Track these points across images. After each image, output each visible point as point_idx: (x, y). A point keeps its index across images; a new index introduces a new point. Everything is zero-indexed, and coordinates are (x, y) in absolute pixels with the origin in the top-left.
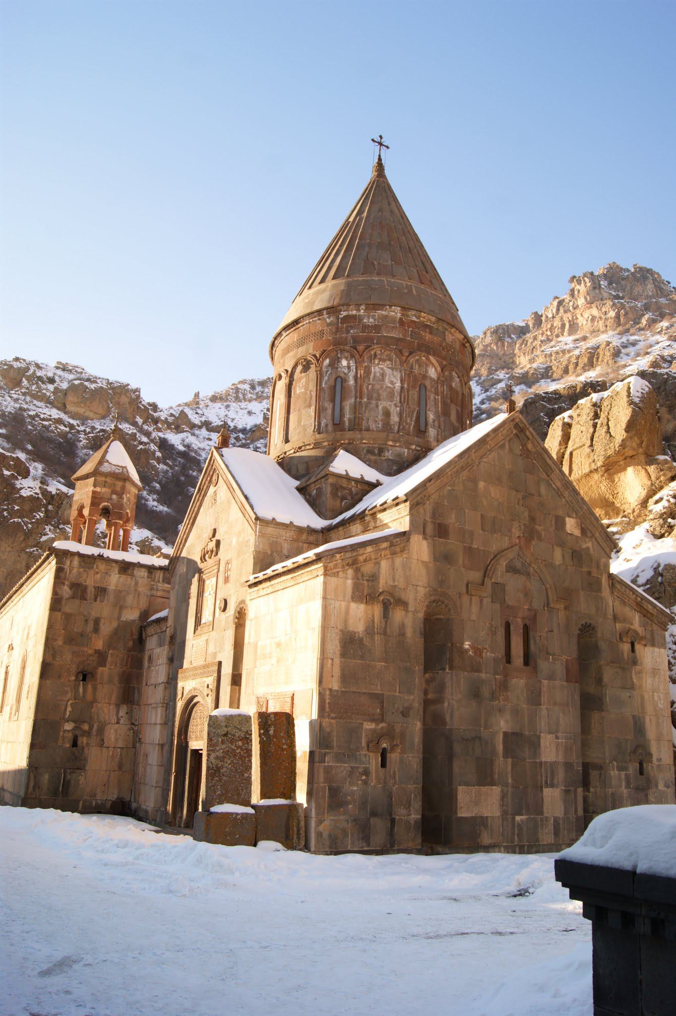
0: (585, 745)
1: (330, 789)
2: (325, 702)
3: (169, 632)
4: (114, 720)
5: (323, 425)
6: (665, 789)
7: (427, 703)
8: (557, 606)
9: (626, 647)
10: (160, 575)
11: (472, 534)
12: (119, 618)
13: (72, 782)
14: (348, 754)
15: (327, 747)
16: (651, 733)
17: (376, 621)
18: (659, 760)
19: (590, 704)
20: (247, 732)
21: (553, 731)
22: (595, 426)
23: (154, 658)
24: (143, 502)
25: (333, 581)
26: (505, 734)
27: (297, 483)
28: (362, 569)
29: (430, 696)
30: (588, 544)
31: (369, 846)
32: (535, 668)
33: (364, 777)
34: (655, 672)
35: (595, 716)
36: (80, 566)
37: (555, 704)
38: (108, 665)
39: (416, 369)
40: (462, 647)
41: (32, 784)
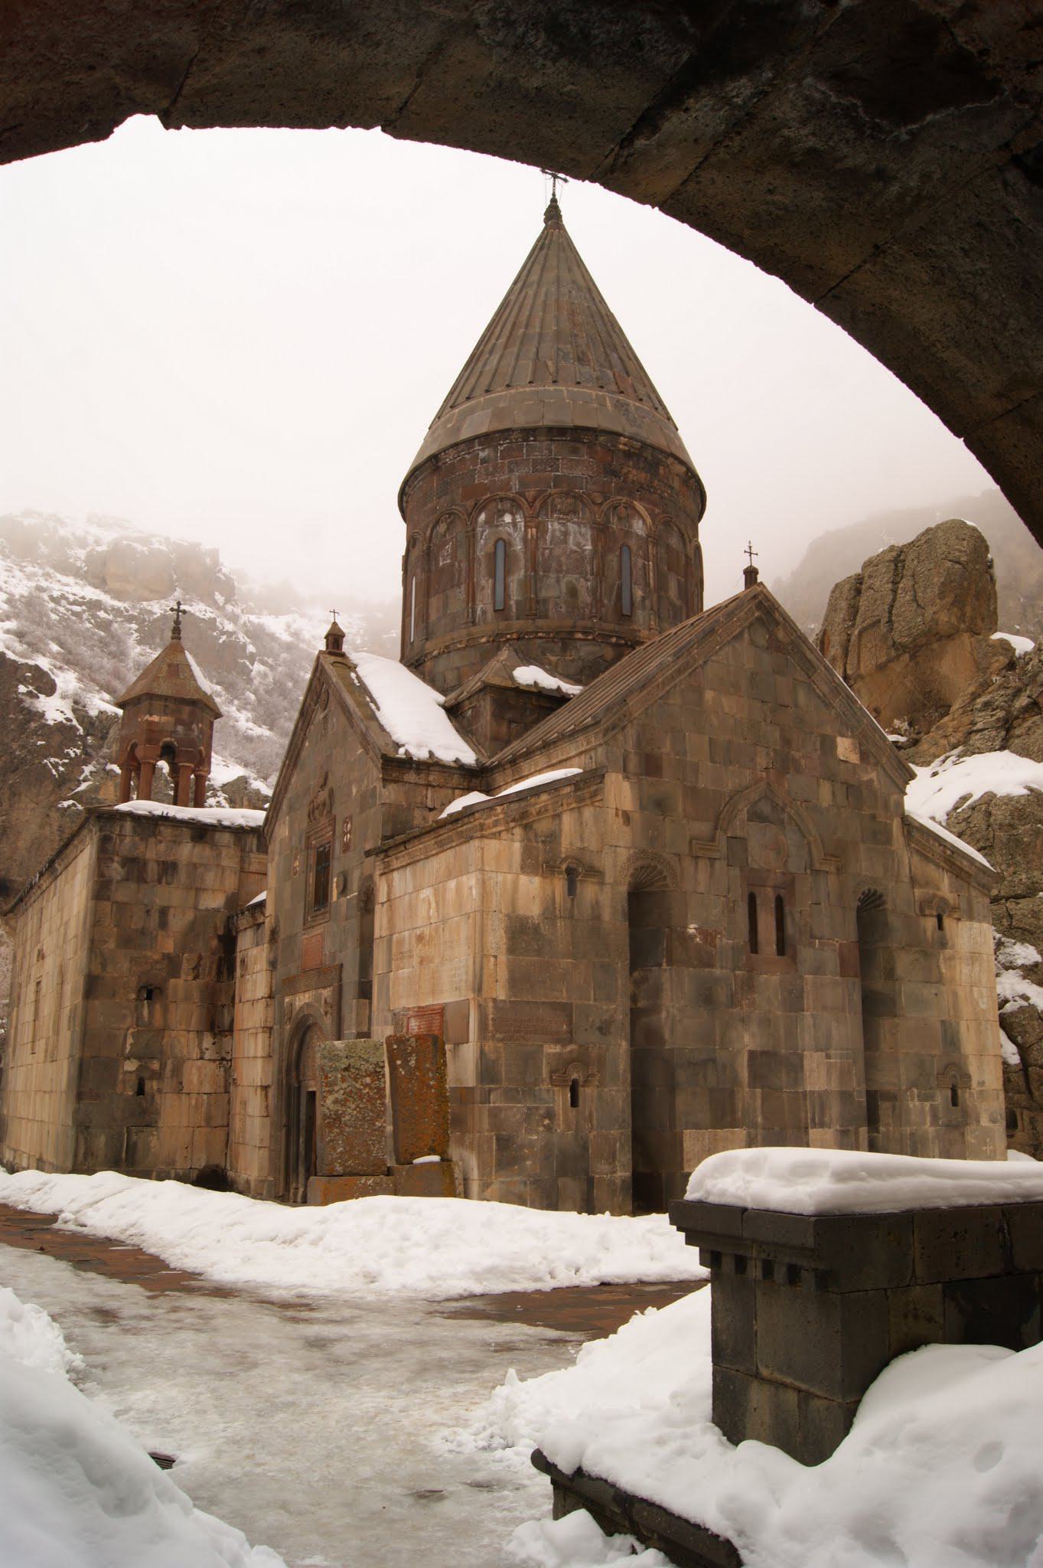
0: (870, 1065)
1: (498, 1140)
2: (486, 1018)
3: (268, 924)
4: (195, 1054)
5: (479, 612)
6: (991, 1125)
7: (635, 1014)
8: (825, 868)
9: (930, 923)
10: (252, 842)
11: (695, 768)
12: (196, 908)
13: (140, 1145)
14: (524, 1088)
15: (492, 1081)
17: (558, 900)
18: (982, 1083)
19: (875, 1007)
20: (377, 1064)
21: (823, 1048)
22: (894, 591)
23: (249, 961)
26: (752, 1054)
27: (442, 699)
28: (535, 826)
29: (641, 1004)
30: (871, 775)
32: (794, 958)
33: (547, 1122)
34: (974, 957)
35: (885, 1025)
36: (135, 832)
37: (824, 1008)
38: (183, 976)
39: (615, 525)
41: (82, 1151)
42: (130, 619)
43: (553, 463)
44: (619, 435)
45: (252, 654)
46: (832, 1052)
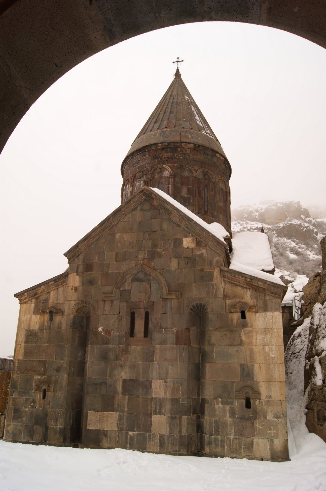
2: (15, 366)
6: (275, 419)
9: (236, 316)
11: (108, 265)
16: (260, 375)
21: (164, 378)
24: (307, 256)
25: (25, 306)
26: (125, 381)
28: (40, 297)
31: (32, 440)
32: (151, 338)
33: (32, 404)
34: (266, 330)
37: (165, 360)
40: (97, 331)
42: (273, 230)
43: (138, 163)
44: (157, 144)
45: (316, 232)
46: (168, 380)
